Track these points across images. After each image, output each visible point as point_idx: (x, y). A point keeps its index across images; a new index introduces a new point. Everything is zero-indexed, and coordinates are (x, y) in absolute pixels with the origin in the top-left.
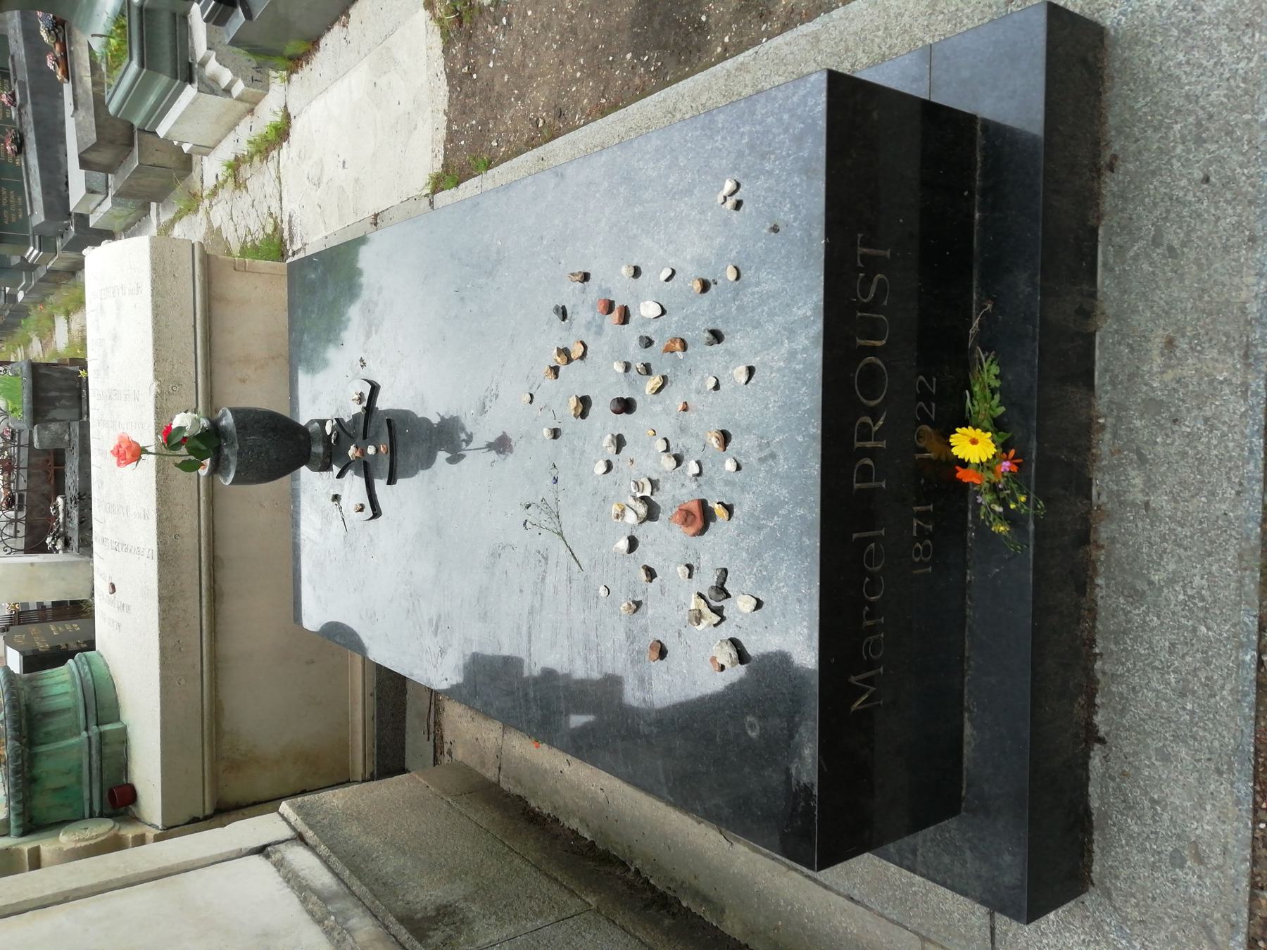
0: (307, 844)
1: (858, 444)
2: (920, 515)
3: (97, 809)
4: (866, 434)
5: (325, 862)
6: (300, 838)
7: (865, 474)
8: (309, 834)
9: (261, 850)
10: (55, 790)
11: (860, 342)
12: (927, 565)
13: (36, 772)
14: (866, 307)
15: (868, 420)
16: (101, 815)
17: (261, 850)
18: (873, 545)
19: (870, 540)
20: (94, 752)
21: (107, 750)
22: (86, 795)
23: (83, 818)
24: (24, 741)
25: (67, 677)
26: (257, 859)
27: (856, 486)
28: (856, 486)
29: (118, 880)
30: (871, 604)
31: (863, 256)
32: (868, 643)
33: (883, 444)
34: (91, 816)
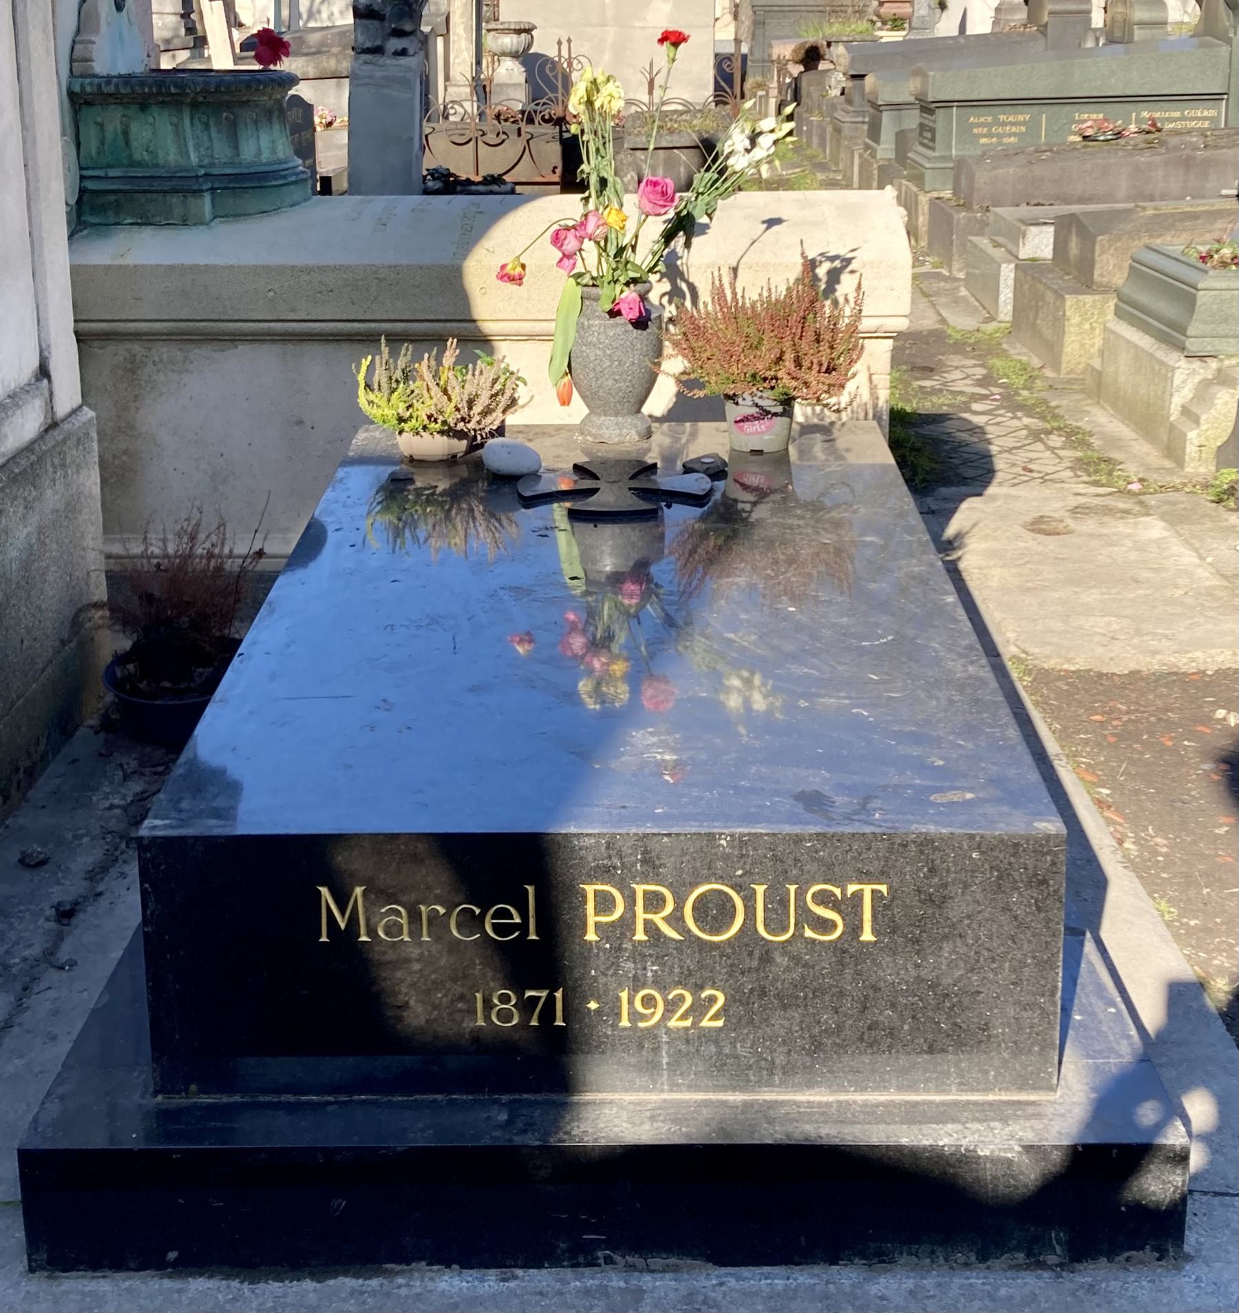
0: (46, 431)
1: (640, 889)
2: (551, 1000)
3: (90, 185)
4: (653, 902)
5: (29, 448)
6: (53, 425)
7: (604, 903)
8: (57, 435)
9: (44, 372)
10: (126, 133)
11: (760, 890)
12: (487, 1018)
13: (155, 111)
14: (802, 907)
15: (669, 908)
16: (82, 191)
17: (44, 372)
18: (518, 920)
19: (525, 916)
20: (175, 182)
21: (175, 200)
22: (112, 173)
23: (81, 168)
24: (200, 99)
25: (281, 155)
26: (36, 364)
27: (590, 889)
28: (590, 889)
29: (37, 189)
30: (448, 914)
31: (858, 896)
32: (398, 913)
33: (640, 936)
34: (82, 178)
